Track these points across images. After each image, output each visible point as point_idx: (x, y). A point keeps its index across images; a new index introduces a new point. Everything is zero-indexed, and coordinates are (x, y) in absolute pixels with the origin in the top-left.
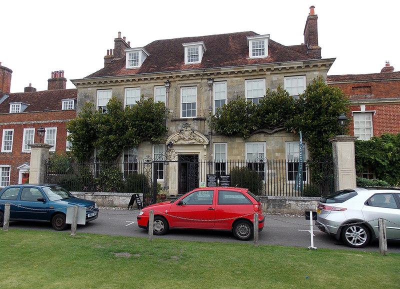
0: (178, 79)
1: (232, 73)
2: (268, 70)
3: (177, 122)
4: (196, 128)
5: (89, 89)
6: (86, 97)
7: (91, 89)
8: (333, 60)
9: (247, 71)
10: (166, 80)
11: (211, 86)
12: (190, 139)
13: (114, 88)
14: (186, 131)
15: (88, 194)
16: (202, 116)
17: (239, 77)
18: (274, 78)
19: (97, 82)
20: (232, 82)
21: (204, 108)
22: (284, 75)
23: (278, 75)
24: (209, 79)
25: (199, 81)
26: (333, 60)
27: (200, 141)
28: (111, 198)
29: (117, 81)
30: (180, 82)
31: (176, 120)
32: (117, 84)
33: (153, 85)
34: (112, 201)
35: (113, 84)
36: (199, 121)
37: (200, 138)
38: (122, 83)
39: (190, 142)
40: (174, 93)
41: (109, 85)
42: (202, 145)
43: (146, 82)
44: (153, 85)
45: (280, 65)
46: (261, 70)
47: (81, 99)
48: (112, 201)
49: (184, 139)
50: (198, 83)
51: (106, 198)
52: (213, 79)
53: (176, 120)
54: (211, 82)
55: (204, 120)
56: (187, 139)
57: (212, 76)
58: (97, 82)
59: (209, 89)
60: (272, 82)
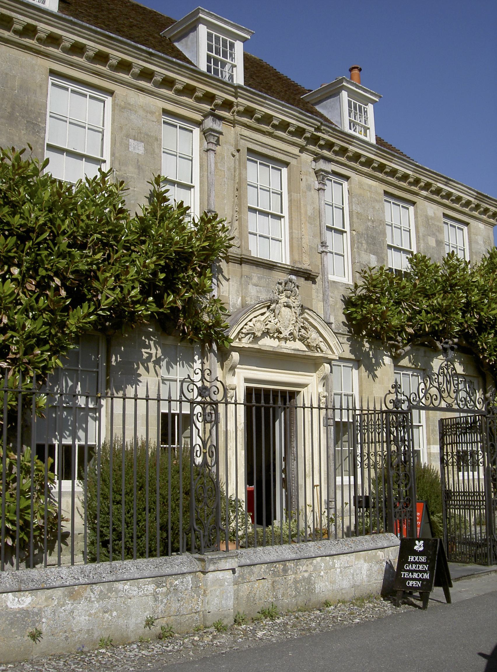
3: (246, 268)
9: (393, 173)
10: (207, 107)
12: (292, 337)
16: (305, 265)
20: (360, 184)
22: (441, 210)
23: (435, 206)
24: (318, 158)
25: (295, 150)
27: (317, 347)
28: (304, 570)
29: (29, 31)
34: (308, 581)
44: (162, 104)
48: (308, 581)
50: (295, 156)
51: (285, 571)
56: (285, 333)
59: (317, 186)
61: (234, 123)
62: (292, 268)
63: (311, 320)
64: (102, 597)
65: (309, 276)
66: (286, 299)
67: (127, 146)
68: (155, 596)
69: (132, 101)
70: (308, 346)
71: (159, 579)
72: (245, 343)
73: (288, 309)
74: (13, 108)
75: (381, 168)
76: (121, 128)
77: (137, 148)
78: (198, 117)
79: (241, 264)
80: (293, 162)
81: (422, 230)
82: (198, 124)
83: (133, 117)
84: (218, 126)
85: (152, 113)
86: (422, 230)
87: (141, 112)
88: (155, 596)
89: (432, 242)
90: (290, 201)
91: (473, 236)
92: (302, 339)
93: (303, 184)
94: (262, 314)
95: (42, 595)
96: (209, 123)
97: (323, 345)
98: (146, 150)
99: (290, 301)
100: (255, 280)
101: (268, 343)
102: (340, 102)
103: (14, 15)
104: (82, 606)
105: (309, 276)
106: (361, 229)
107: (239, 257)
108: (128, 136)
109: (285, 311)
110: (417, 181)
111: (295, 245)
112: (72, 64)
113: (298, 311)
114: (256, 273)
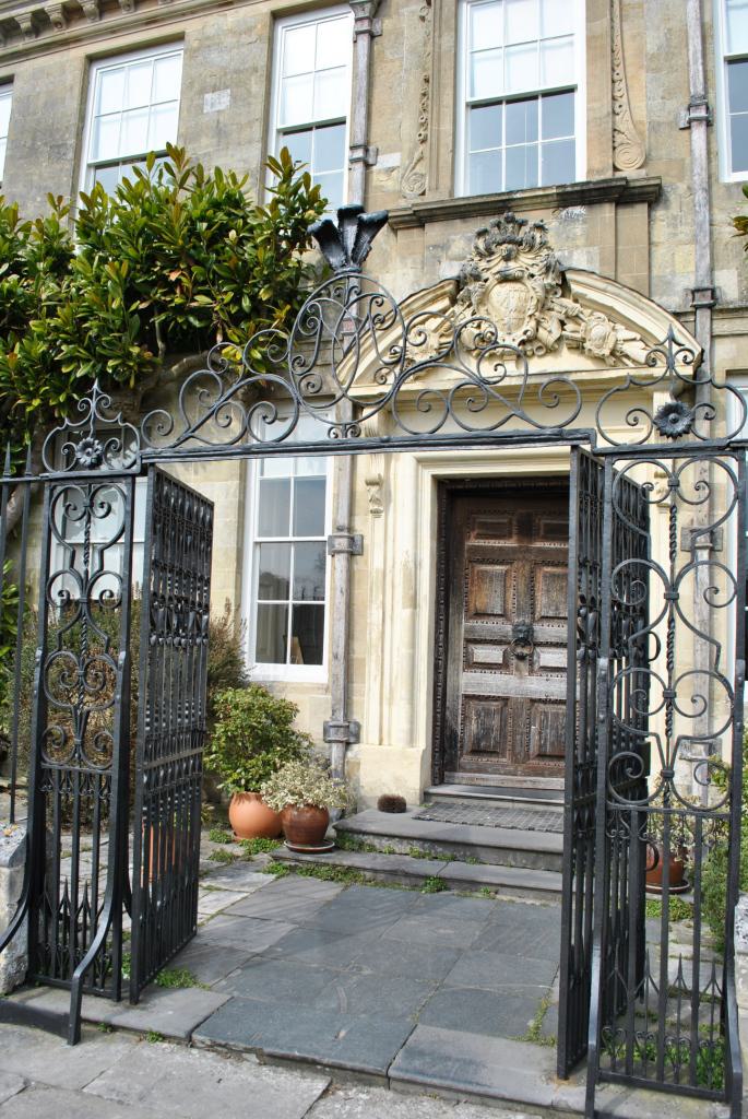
3: (434, 232)
4: (579, 260)
12: (530, 346)
14: (505, 279)
16: (631, 172)
21: (641, 113)
27: (617, 355)
32: (47, 37)
35: (20, 45)
36: (607, 211)
37: (623, 333)
39: (538, 365)
49: (487, 346)
55: (651, 196)
56: (511, 339)
62: (560, 191)
63: (592, 295)
66: (502, 266)
67: (201, 107)
69: (210, 31)
70: (601, 359)
73: (508, 286)
74: (34, 139)
79: (422, 226)
83: (214, 57)
85: (249, 31)
87: (229, 40)
92: (578, 347)
94: (444, 311)
98: (234, 98)
99: (513, 267)
103: (13, 13)
107: (411, 212)
108: (203, 91)
111: (609, 135)
112: (113, 31)
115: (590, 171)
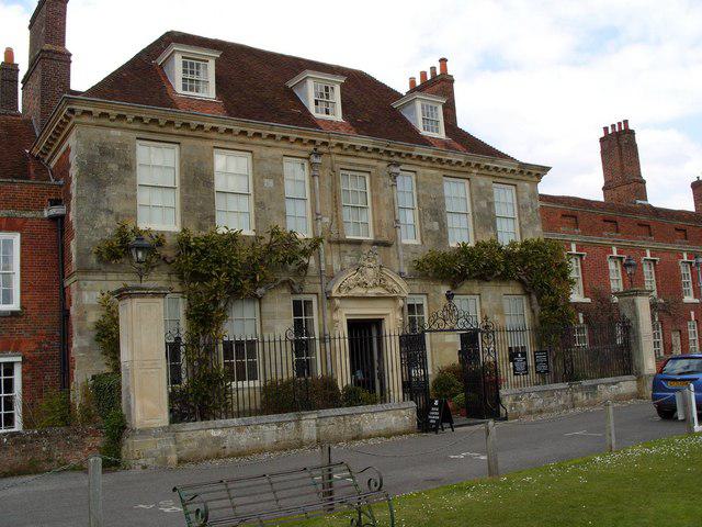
0: (338, 150)
1: (429, 159)
2: (478, 166)
3: (343, 247)
5: (113, 132)
6: (104, 151)
7: (119, 133)
8: (549, 169)
9: (449, 162)
10: (311, 148)
11: (394, 176)
12: (375, 285)
13: (185, 141)
15: (309, 417)
16: (385, 238)
17: (436, 168)
18: (482, 181)
19: (147, 118)
22: (492, 179)
23: (486, 179)
24: (391, 164)
25: (374, 163)
26: (549, 169)
27: (393, 291)
28: (355, 420)
30: (339, 158)
31: (339, 242)
33: (281, 152)
35: (187, 133)
38: (208, 135)
40: (328, 180)
41: (176, 132)
42: (394, 299)
43: (270, 142)
44: (281, 152)
45: (493, 161)
46: (469, 164)
47: (91, 158)
50: (373, 167)
52: (397, 165)
53: (339, 242)
54: (396, 170)
57: (397, 159)
58: (147, 118)
60: (480, 188)
61: (330, 154)
64: (252, 431)
65: (386, 245)
68: (277, 431)
71: (279, 424)
72: (343, 294)
75: (440, 160)
76: (258, 173)
77: (269, 183)
78: (306, 155)
80: (373, 171)
81: (475, 197)
82: (308, 159)
83: (266, 164)
84: (318, 160)
86: (475, 197)
88: (277, 431)
89: (484, 204)
90: (372, 197)
91: (520, 195)
92: (383, 287)
93: (381, 185)
95: (226, 431)
96: (313, 159)
97: (396, 289)
100: (349, 253)
101: (360, 291)
102: (415, 108)
104: (243, 435)
105: (386, 245)
106: (426, 206)
109: (370, 271)
110: (469, 164)
111: (378, 225)
113: (378, 269)
114: (349, 249)
115: (376, 236)
